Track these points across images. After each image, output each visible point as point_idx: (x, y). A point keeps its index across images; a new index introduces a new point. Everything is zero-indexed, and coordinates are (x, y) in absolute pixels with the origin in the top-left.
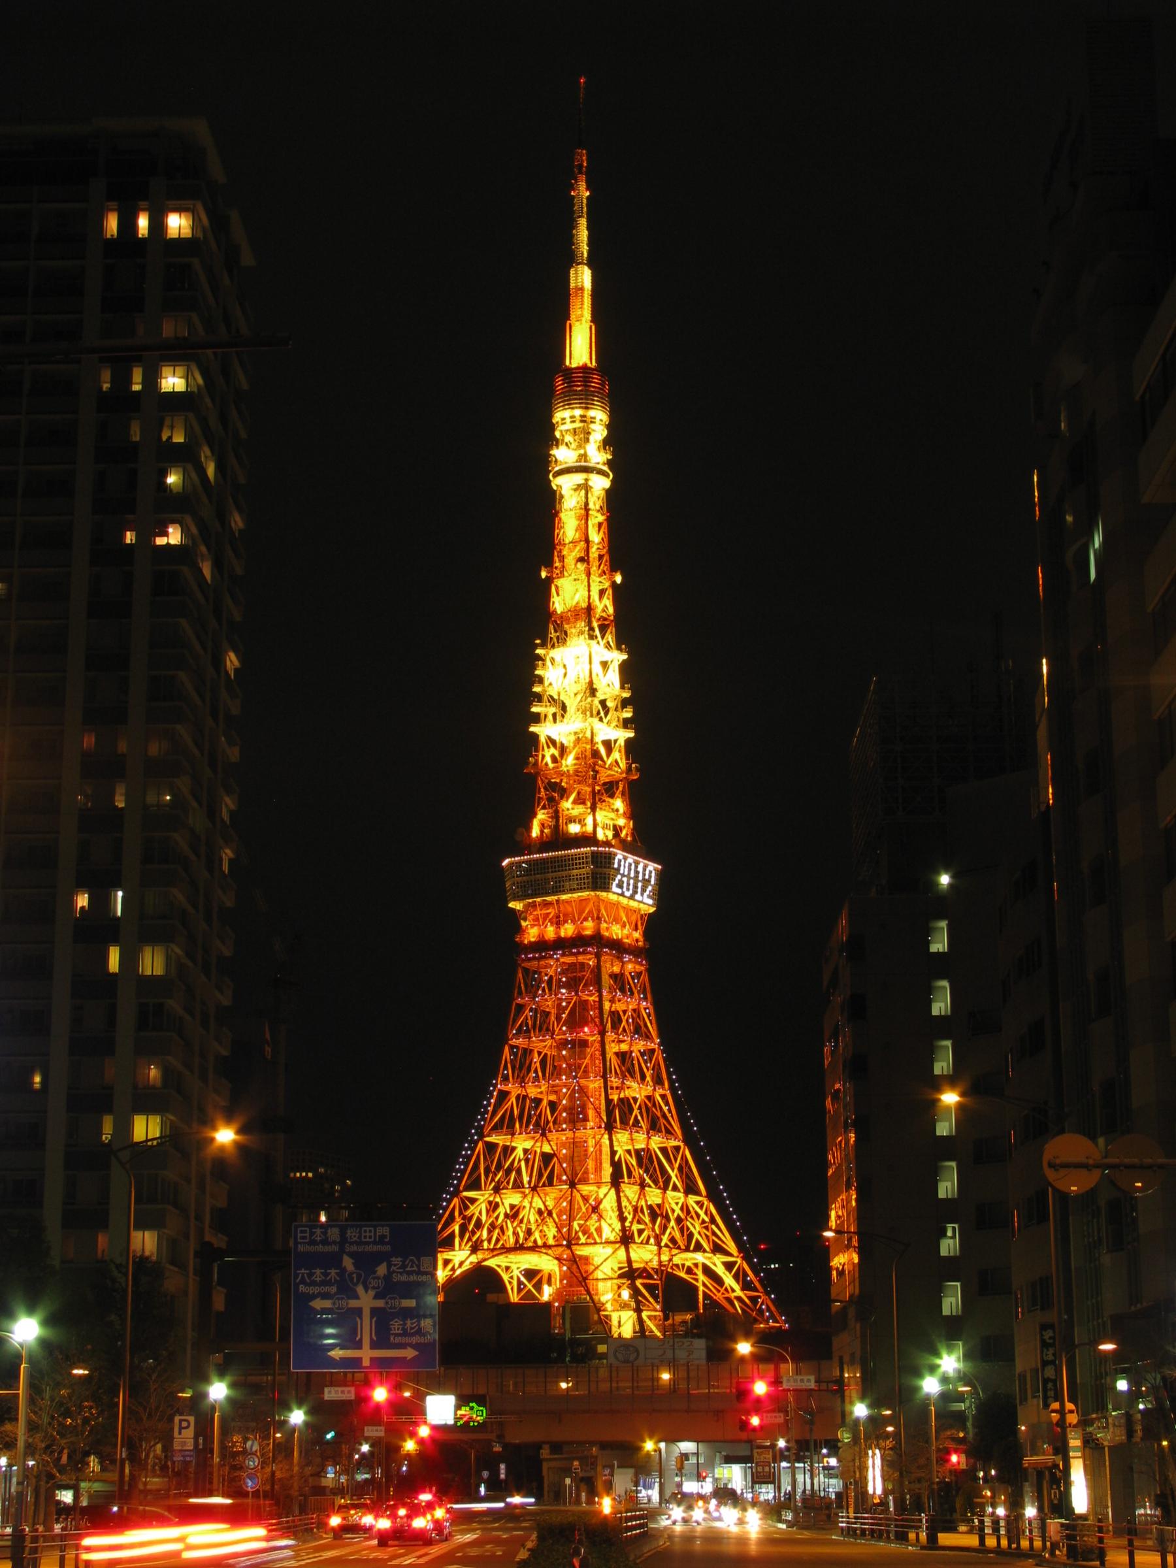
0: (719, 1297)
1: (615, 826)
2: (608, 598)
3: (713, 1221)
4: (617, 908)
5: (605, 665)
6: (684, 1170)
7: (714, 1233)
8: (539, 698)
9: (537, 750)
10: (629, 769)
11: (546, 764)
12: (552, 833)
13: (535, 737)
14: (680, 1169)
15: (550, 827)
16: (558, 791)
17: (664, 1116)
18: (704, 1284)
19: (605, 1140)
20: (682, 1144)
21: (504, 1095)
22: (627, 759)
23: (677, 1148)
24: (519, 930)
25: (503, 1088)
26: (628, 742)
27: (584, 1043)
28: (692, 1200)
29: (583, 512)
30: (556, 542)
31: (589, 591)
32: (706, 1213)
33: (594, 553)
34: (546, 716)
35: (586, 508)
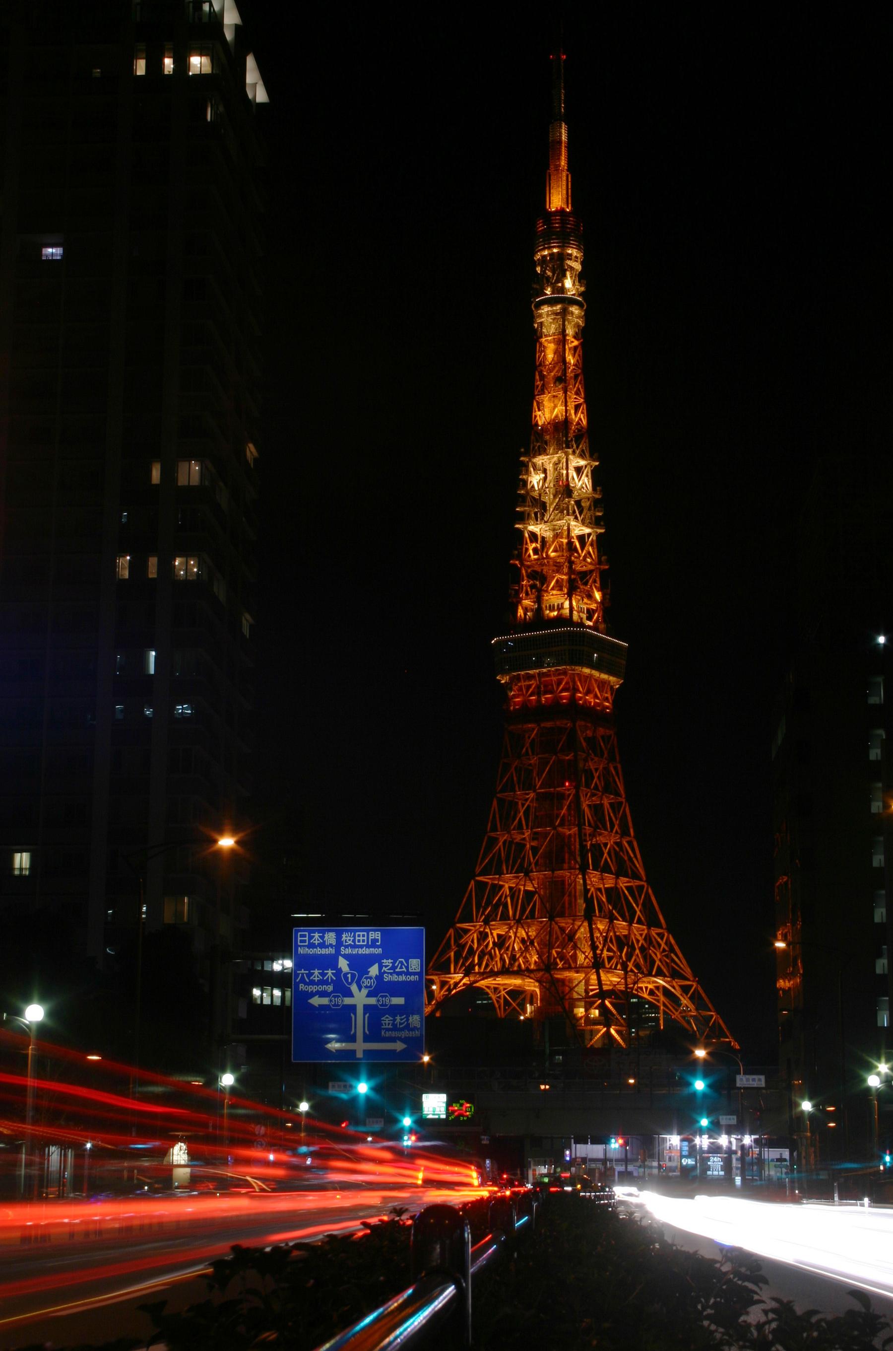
0: (676, 1015)
1: (588, 610)
2: (587, 476)
3: (672, 950)
4: (590, 681)
5: (579, 470)
6: (647, 907)
7: (673, 960)
8: (523, 499)
9: (522, 544)
10: (600, 562)
11: (529, 556)
12: (534, 615)
13: (520, 533)
14: (644, 905)
15: (532, 610)
16: (540, 579)
17: (630, 859)
18: (664, 1004)
19: (594, 977)
20: (645, 884)
21: (493, 841)
22: (599, 552)
23: (641, 888)
24: (507, 700)
25: (492, 834)
26: (599, 536)
27: (562, 797)
28: (654, 932)
29: (561, 337)
30: (538, 364)
31: (566, 406)
32: (666, 943)
33: (570, 373)
34: (529, 514)
35: (563, 333)
